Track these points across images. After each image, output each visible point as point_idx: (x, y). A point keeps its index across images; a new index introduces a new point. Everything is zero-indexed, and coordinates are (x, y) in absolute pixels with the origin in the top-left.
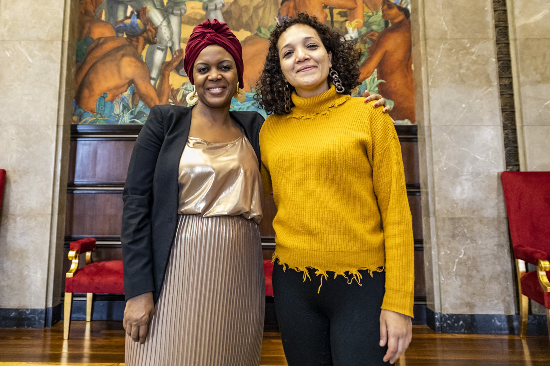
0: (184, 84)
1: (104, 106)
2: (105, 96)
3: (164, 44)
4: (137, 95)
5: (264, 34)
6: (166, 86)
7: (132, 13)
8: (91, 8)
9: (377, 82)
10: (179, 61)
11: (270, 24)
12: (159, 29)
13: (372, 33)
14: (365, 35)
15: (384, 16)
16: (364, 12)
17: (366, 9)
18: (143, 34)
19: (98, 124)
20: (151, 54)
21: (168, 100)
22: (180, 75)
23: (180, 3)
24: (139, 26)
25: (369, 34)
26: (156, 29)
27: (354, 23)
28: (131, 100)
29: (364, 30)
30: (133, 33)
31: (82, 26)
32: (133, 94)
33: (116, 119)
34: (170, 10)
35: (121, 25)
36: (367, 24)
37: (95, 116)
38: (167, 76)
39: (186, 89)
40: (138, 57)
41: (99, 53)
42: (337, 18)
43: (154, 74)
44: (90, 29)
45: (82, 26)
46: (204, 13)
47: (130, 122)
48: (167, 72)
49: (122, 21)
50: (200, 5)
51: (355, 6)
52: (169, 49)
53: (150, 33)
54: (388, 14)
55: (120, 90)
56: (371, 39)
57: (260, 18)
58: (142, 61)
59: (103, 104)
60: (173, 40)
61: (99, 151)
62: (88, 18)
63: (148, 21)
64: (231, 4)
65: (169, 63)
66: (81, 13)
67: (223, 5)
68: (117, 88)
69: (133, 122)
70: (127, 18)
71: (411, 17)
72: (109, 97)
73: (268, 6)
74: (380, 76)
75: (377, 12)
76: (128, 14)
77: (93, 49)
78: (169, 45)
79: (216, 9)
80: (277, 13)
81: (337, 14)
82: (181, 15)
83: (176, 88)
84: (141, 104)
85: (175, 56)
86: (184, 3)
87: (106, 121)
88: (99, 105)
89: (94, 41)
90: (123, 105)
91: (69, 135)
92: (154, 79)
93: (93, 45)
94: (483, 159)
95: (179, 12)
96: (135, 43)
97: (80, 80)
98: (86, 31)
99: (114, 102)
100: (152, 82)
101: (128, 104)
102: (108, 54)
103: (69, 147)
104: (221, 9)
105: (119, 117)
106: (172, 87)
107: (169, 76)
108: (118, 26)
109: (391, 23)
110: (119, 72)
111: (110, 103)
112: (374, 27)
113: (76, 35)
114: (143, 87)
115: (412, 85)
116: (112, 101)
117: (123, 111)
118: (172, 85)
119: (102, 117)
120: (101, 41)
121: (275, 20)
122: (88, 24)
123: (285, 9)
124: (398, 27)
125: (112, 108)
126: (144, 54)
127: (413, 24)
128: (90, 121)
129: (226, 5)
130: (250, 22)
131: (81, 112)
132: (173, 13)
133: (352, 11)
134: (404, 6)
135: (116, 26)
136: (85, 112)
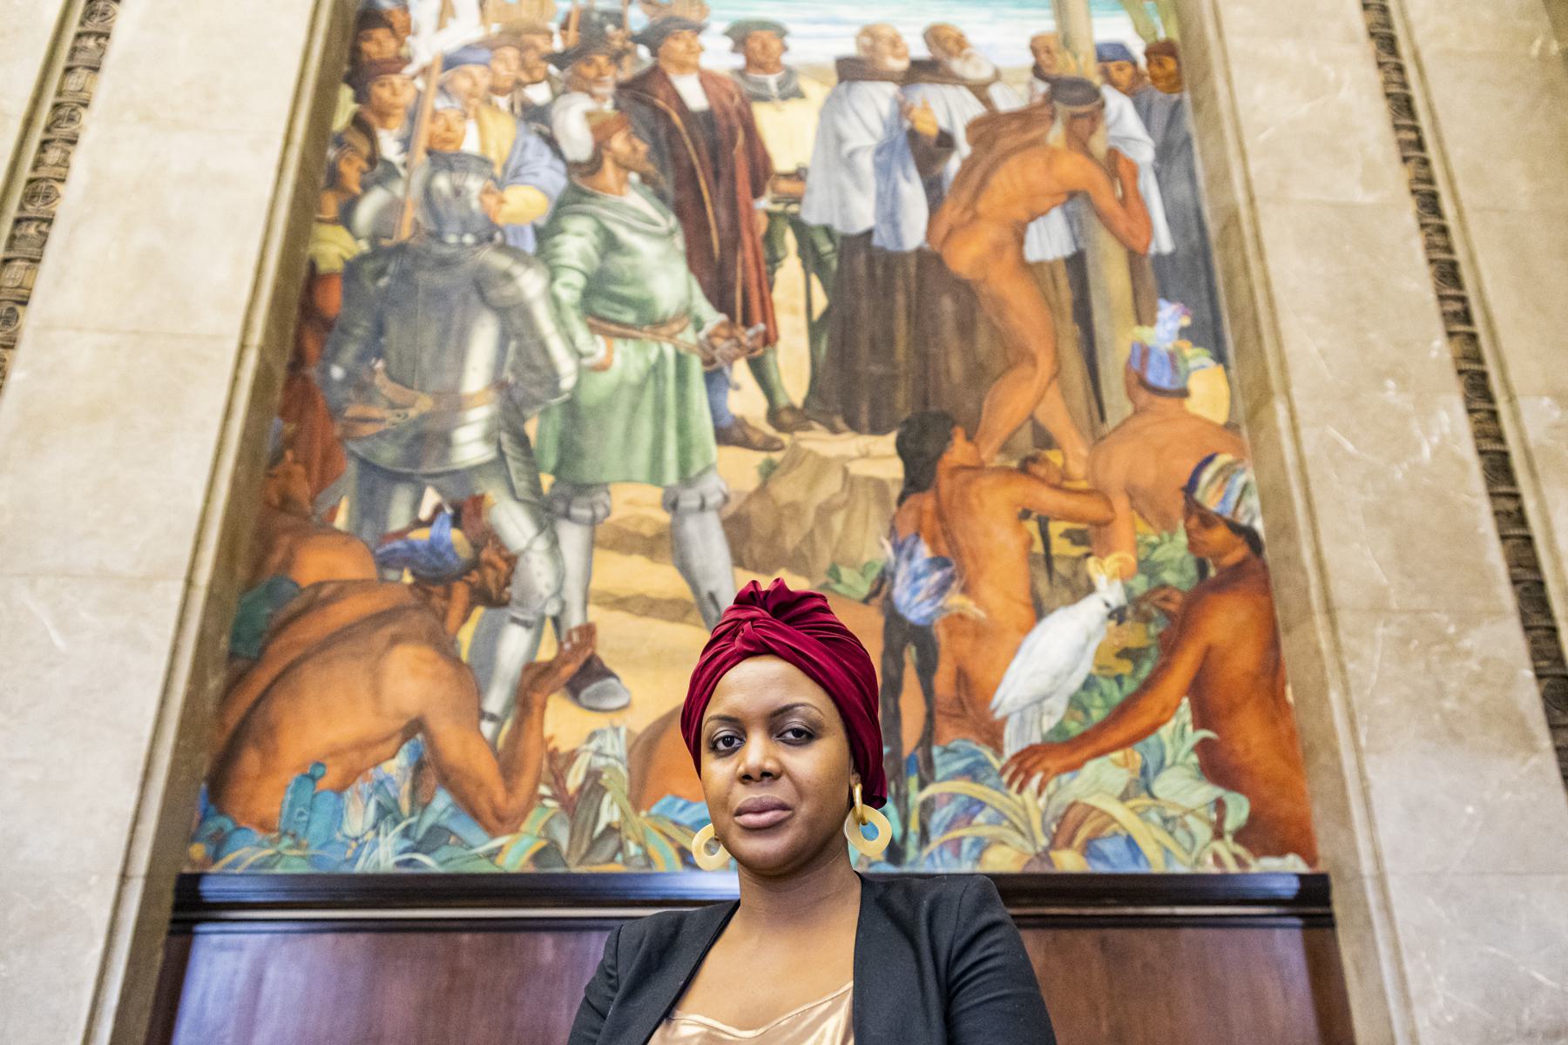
1: (311, 808)
2: (318, 772)
3: (536, 606)
4: (431, 769)
5: (849, 587)
6: (531, 743)
7: (438, 510)
8: (301, 490)
9: (1194, 736)
10: (581, 661)
11: (866, 558)
12: (521, 563)
13: (1164, 593)
14: (1144, 598)
15: (1192, 546)
16: (1136, 533)
17: (1141, 526)
18: (468, 573)
19: (279, 870)
20: (489, 640)
22: (580, 705)
23: (589, 486)
24: (458, 549)
25: (1158, 596)
26: (512, 560)
27: (1111, 562)
28: (407, 786)
29: (1140, 584)
30: (436, 569)
31: (265, 541)
32: (419, 767)
33: (349, 854)
34: (560, 507)
35: (398, 544)
36: (1147, 567)
37: (272, 843)
38: (536, 710)
39: (599, 753)
40: (445, 647)
41: (312, 630)
42: (1060, 547)
43: (495, 701)
44: (291, 553)
45: (265, 541)
46: (665, 518)
47: (398, 864)
48: (538, 697)
49: (401, 535)
50: (655, 494)
51: (1109, 515)
52: (549, 625)
53: (490, 573)
54: (1205, 543)
55: (372, 755)
56: (1162, 610)
57: (835, 540)
58: (456, 661)
59: (307, 800)
60: (566, 596)
61: (272, 973)
62: (290, 520)
63: (487, 538)
64: (750, 497)
65: (548, 669)
66: (268, 503)
67: (726, 499)
68: (363, 745)
69: (409, 862)
70: (419, 524)
71: (1267, 554)
72: (333, 775)
73: (861, 506)
74: (1201, 721)
75: (1172, 534)
76: (425, 513)
77: (293, 618)
78: (552, 609)
79: (703, 507)
80: (887, 526)
81: (1061, 535)
82: (593, 522)
83: (564, 748)
84: (442, 801)
85: (567, 646)
86: (604, 486)
87: (311, 860)
88: (292, 805)
89: (302, 591)
90: (379, 804)
91: (164, 912)
92: (492, 718)
93: (295, 605)
94: (1554, 985)
95: (587, 513)
96: (437, 601)
97: (233, 719)
98: (277, 558)
99: (348, 793)
100: (487, 728)
101: (395, 801)
102: (345, 634)
103: (159, 957)
104: (719, 509)
105: (361, 846)
106: (551, 746)
107: (544, 707)
108: (388, 547)
109: (1216, 565)
110: (376, 692)
111: (332, 797)
112: (1169, 577)
113: (242, 572)
114: (454, 743)
115: (1297, 749)
116: (340, 791)
117: (375, 827)
118: (551, 738)
119: (297, 846)
120: (325, 592)
121: (882, 546)
122: (285, 540)
123: (910, 516)
124: (1234, 577)
125: (338, 816)
126: (466, 636)
127: (1278, 572)
128: (251, 860)
129: (733, 497)
130: (805, 550)
131: (221, 829)
132: (567, 516)
133: (1103, 530)
134: (1244, 521)
135: (380, 545)
136: (238, 829)
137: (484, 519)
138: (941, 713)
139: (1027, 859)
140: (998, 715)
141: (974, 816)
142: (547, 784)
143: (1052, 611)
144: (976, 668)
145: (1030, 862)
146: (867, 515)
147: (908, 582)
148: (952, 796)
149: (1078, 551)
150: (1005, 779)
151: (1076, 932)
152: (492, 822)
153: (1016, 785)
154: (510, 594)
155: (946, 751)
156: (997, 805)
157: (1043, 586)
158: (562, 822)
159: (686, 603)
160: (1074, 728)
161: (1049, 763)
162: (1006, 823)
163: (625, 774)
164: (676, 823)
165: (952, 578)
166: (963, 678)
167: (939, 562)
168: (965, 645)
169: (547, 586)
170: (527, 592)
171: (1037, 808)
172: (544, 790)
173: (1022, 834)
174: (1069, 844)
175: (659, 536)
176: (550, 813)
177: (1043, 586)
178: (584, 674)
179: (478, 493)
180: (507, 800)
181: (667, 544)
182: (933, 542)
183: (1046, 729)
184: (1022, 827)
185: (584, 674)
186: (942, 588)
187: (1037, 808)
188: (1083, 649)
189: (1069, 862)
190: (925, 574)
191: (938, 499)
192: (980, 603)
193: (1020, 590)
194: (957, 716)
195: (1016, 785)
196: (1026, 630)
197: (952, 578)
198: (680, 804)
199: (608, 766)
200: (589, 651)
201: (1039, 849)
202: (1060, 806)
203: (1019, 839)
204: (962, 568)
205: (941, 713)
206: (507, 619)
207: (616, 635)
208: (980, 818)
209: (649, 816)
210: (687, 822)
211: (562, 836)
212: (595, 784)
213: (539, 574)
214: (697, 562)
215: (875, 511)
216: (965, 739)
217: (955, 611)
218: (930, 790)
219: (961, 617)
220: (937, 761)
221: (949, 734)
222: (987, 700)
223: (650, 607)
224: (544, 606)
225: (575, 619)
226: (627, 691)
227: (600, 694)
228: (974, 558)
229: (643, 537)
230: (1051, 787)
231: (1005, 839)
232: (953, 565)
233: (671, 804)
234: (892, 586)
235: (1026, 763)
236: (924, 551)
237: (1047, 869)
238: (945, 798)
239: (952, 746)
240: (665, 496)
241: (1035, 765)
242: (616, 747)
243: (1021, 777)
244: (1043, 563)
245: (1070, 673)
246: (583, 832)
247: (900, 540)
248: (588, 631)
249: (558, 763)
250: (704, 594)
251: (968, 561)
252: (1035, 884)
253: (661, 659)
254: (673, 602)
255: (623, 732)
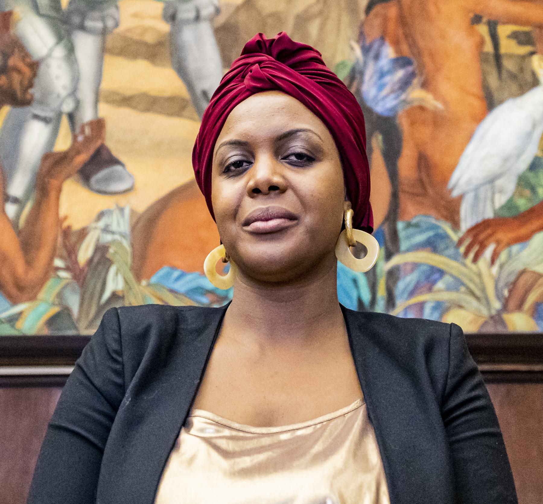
0: (101, 215)
6: (49, 220)
21: (51, 259)
38: (53, 194)
39: (106, 230)
43: (18, 186)
48: (54, 183)
52: (65, 121)
67: (218, 11)
79: (197, 18)
83: (77, 226)
85: (80, 138)
92: (16, 200)
104: (211, 19)
106: (65, 224)
107: (59, 190)
118: (66, 218)
137: (12, 32)
138: (404, 192)
139: (481, 321)
140: (455, 194)
141: (434, 282)
142: (61, 257)
143: (501, 102)
144: (435, 153)
145: (486, 323)
146: (339, 20)
147: (375, 78)
148: (415, 266)
149: (524, 50)
150: (462, 249)
151: (527, 385)
152: (13, 291)
153: (471, 255)
154: (32, 96)
155: (409, 225)
156: (455, 273)
157: (493, 81)
158: (74, 291)
159: (183, 100)
160: (523, 204)
161: (501, 235)
162: (463, 289)
163: (129, 249)
164: (172, 291)
165: (413, 75)
166: (423, 162)
167: (401, 61)
168: (425, 133)
169: (64, 88)
170: (47, 93)
171: (491, 275)
172: (58, 263)
173: (478, 299)
174: (520, 307)
175: (160, 44)
176: (64, 283)
177: (493, 81)
178: (95, 161)
179: (7, 9)
180: (26, 272)
181: (166, 50)
182: (396, 44)
183: (497, 205)
184: (478, 293)
185: (95, 161)
186: (405, 84)
187: (491, 275)
188: (529, 135)
189: (520, 323)
190: (390, 72)
191: (401, 8)
192: (437, 95)
193: (473, 84)
194: (418, 195)
195: (471, 255)
196: (479, 119)
197: (413, 75)
198: (176, 274)
199: (114, 241)
200: (99, 143)
201: (494, 312)
202: (510, 274)
203: (474, 303)
204: (422, 66)
205: (404, 192)
206: (30, 115)
207: (122, 127)
208: (440, 285)
209: (149, 285)
210: (182, 290)
211: (74, 302)
212: (102, 258)
213: (57, 77)
214: (192, 64)
215: (346, 19)
216: (426, 215)
217: (416, 104)
218: (396, 260)
219: (422, 108)
220: (402, 234)
221: (411, 210)
222: (445, 180)
223: (151, 103)
224: (61, 105)
225: (87, 115)
226: (130, 176)
227: (108, 179)
228: (432, 55)
229: (146, 44)
230: (503, 256)
231: (463, 304)
232: (415, 64)
233: (168, 275)
234: (361, 82)
235: (481, 234)
236: (389, 52)
237: (500, 330)
238: (409, 268)
239: (414, 221)
240: (165, 10)
241: (490, 236)
242: (121, 225)
243: (476, 248)
244: (492, 59)
245: (519, 156)
246: (91, 298)
247: (368, 42)
248: (98, 125)
249: (71, 240)
250: (198, 92)
251: (427, 59)
252: (487, 343)
253: (161, 148)
254: (171, 99)
255: (127, 212)
